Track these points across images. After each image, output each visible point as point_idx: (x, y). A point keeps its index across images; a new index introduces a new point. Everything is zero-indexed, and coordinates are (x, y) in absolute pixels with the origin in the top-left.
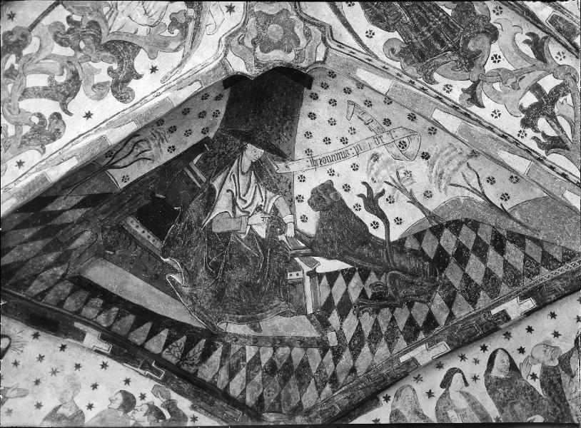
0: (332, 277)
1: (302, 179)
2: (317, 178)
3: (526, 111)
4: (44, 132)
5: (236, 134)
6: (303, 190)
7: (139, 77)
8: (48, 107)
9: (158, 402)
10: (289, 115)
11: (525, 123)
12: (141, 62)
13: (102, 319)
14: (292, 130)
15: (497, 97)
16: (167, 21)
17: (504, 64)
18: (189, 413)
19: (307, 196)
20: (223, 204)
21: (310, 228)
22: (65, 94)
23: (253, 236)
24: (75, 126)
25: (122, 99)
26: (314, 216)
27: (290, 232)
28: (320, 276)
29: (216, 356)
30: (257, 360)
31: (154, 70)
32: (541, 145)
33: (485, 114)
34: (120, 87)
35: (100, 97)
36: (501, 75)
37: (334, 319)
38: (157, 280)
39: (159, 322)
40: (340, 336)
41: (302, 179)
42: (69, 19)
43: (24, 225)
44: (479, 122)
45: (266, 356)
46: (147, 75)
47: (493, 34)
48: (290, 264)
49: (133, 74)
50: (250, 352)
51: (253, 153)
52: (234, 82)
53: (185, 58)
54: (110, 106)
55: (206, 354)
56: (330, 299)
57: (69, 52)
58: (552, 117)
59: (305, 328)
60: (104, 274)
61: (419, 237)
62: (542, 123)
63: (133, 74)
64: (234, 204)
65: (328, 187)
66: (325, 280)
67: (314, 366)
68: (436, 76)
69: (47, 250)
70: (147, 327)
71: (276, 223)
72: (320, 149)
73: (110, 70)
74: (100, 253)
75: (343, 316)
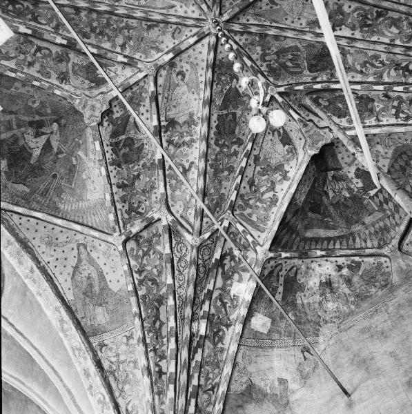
0: (376, 195)
1: (349, 172)
2: (353, 169)
3: (395, 115)
4: (274, 201)
5: (323, 171)
6: (351, 175)
7: (288, 172)
8: (270, 194)
9: (349, 263)
10: (334, 156)
11: (397, 118)
12: (287, 168)
13: (318, 247)
14: (338, 161)
15: (383, 116)
16: (286, 153)
17: (381, 106)
18: (360, 260)
19: (354, 176)
20: (331, 194)
21: (360, 185)
22: (273, 188)
23: (345, 198)
24: (280, 195)
25: (288, 180)
26: (359, 181)
27: (356, 190)
28: (373, 197)
29: (358, 240)
30: (370, 233)
31: (291, 167)
32: (405, 121)
33: (385, 123)
34: (285, 177)
35: (282, 183)
36: (383, 110)
37: (385, 205)
38: (327, 227)
39: (334, 239)
40: (390, 210)
41: (349, 172)
42: (261, 168)
43: (283, 228)
44: (384, 126)
45: (372, 230)
46: (291, 170)
47: (373, 100)
48: (361, 199)
49: (286, 172)
50: (367, 232)
51: (330, 174)
52: (314, 158)
53: (297, 159)
54: (286, 184)
55: (354, 240)
56: (380, 202)
57: (266, 177)
58: (403, 112)
59: (380, 215)
60: (309, 234)
61: (393, 166)
62: (401, 115)
63: (286, 172)
64: (334, 191)
65: (358, 169)
66: (375, 197)
67: (388, 224)
68: (365, 121)
69: (292, 234)
70: (332, 242)
71: (350, 190)
72: (348, 160)
73: (280, 175)
74: (306, 228)
75: (387, 204)
